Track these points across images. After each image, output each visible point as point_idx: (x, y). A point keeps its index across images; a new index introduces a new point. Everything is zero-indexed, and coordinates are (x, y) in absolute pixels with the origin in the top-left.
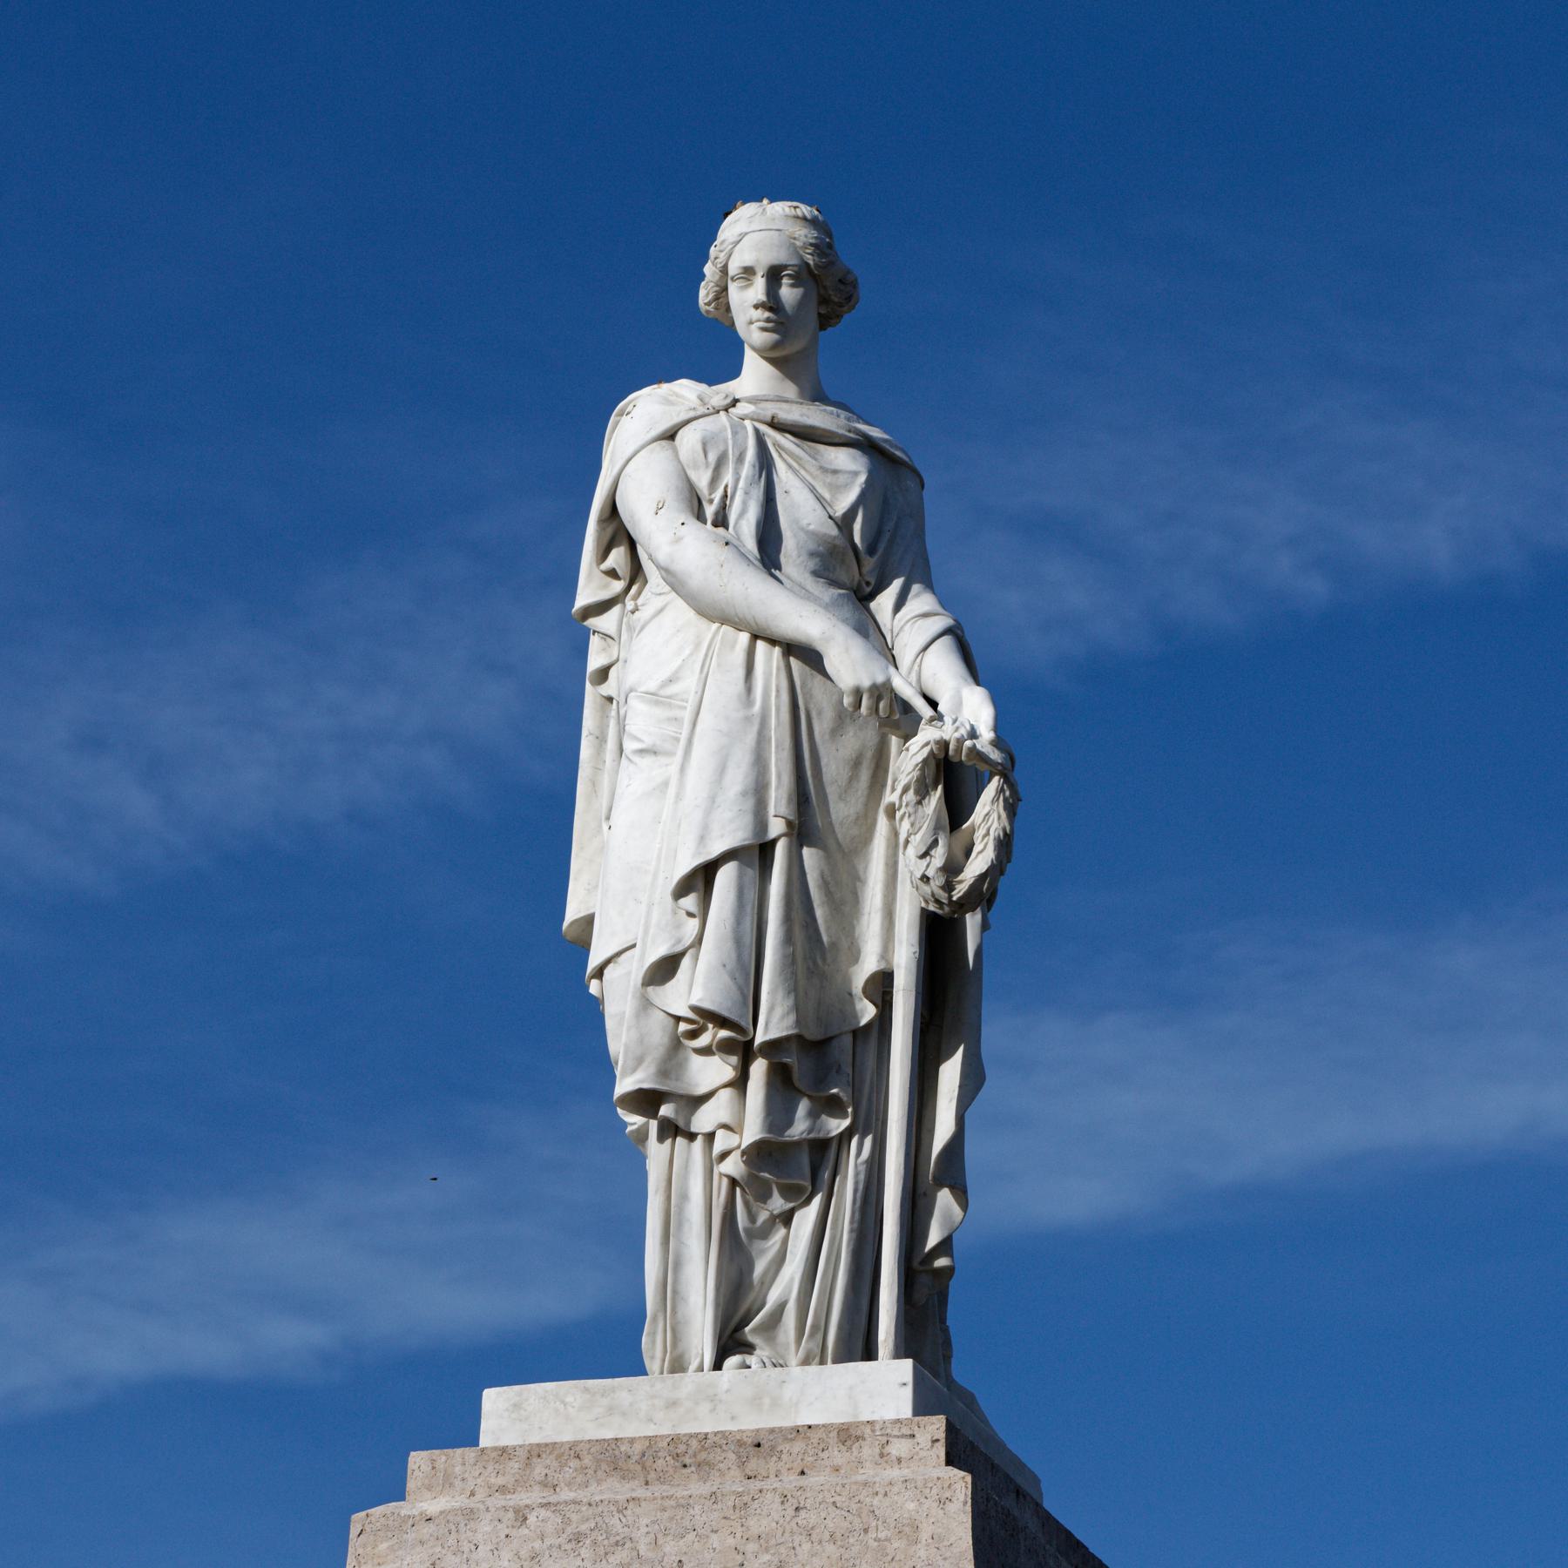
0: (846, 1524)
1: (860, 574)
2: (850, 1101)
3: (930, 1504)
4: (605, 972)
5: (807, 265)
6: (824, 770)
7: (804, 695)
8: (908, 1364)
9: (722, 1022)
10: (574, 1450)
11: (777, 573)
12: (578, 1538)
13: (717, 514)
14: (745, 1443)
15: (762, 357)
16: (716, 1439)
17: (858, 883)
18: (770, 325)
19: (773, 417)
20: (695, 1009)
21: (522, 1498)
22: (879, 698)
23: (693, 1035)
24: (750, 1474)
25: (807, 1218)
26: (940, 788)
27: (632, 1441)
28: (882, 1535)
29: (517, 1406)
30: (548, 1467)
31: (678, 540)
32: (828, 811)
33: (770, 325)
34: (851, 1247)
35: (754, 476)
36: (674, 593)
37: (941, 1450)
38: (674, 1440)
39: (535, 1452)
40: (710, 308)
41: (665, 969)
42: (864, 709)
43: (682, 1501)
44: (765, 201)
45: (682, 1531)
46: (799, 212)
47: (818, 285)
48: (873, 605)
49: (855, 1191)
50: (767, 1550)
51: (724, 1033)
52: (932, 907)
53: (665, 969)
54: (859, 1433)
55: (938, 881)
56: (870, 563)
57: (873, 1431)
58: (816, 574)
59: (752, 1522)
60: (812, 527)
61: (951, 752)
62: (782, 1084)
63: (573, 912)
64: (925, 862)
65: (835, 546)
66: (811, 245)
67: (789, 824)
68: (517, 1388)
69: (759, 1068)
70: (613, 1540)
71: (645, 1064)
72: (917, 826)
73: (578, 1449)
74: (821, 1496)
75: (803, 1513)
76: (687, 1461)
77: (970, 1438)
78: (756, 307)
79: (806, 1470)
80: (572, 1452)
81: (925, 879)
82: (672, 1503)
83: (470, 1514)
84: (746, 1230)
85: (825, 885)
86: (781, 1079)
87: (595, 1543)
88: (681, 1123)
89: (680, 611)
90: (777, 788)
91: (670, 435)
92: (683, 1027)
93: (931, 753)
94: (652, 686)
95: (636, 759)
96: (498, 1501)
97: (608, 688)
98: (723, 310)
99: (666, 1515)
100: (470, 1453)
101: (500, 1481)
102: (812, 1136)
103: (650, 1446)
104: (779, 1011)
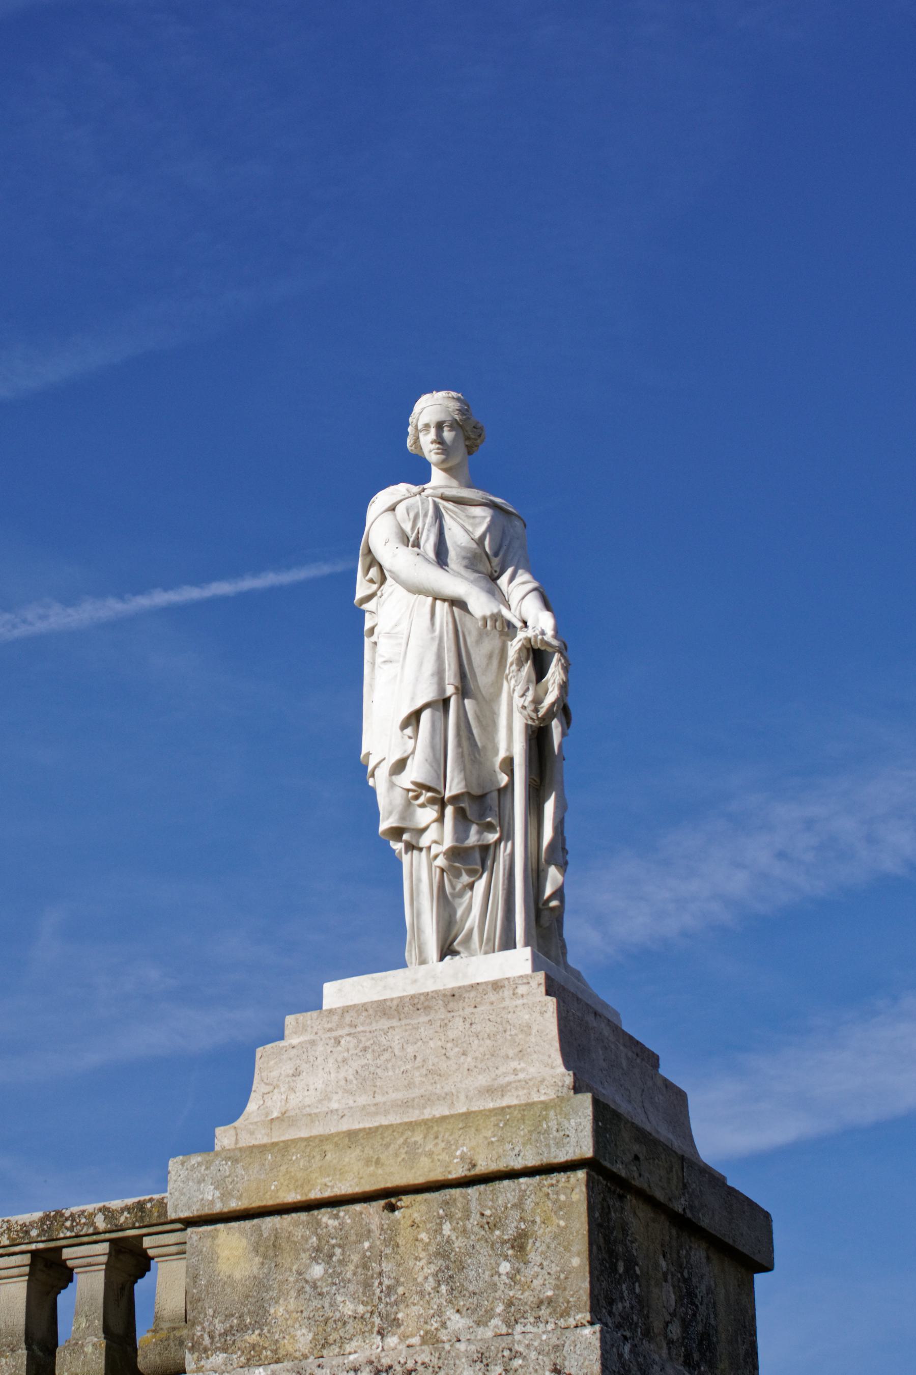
0: (495, 1029)
1: (491, 567)
2: (498, 824)
3: (536, 1015)
4: (375, 773)
5: (456, 420)
6: (473, 661)
7: (461, 625)
8: (529, 949)
9: (429, 789)
10: (364, 1007)
11: (446, 568)
12: (365, 1049)
13: (414, 541)
14: (447, 995)
15: (439, 469)
16: (433, 994)
17: (495, 716)
18: (440, 451)
19: (442, 494)
20: (415, 783)
21: (340, 1032)
22: (496, 621)
23: (417, 797)
24: (450, 1010)
25: (480, 885)
26: (529, 662)
27: (392, 1000)
28: (513, 1033)
29: (340, 990)
30: (352, 1017)
31: (395, 556)
32: (477, 681)
33: (440, 451)
34: (504, 897)
35: (432, 522)
36: (397, 584)
37: (543, 989)
38: (412, 997)
39: (346, 1010)
40: (413, 448)
41: (400, 766)
42: (489, 627)
43: (416, 1026)
44: (434, 392)
45: (415, 1040)
46: (450, 395)
47: (463, 430)
48: (499, 582)
49: (504, 869)
50: (457, 1046)
51: (430, 794)
52: (530, 722)
53: (400, 766)
54: (502, 984)
55: (531, 707)
56: (496, 561)
57: (509, 982)
58: (467, 567)
59: (449, 1033)
60: (463, 545)
61: (533, 643)
62: (462, 816)
63: (364, 751)
64: (523, 699)
65: (476, 553)
66: (457, 410)
67: (457, 688)
68: (339, 981)
69: (449, 810)
70: (382, 1048)
71: (393, 815)
72: (518, 682)
73: (366, 1006)
74: (482, 1016)
75: (474, 1026)
76: (419, 1006)
77: (562, 984)
78: (432, 443)
79: (477, 1005)
80: (363, 1009)
81: (524, 707)
82: (410, 1027)
83: (313, 1043)
84: (452, 894)
85: (478, 718)
86: (461, 814)
87: (373, 1051)
88: (414, 843)
89: (401, 591)
90: (449, 670)
91: (393, 509)
92: (411, 794)
93: (523, 645)
94: (387, 630)
95: (383, 666)
96: (329, 1034)
97: (373, 639)
98: (419, 448)
99: (407, 1033)
100: (315, 1014)
101: (329, 1026)
102: (480, 843)
103: (401, 1001)
104: (456, 781)
